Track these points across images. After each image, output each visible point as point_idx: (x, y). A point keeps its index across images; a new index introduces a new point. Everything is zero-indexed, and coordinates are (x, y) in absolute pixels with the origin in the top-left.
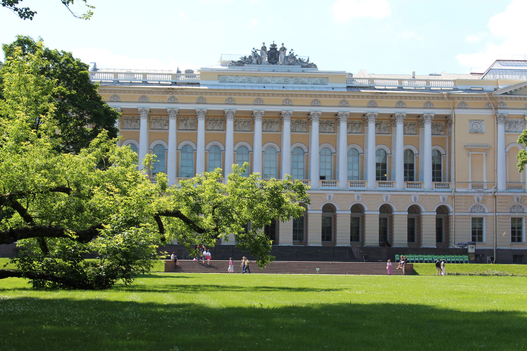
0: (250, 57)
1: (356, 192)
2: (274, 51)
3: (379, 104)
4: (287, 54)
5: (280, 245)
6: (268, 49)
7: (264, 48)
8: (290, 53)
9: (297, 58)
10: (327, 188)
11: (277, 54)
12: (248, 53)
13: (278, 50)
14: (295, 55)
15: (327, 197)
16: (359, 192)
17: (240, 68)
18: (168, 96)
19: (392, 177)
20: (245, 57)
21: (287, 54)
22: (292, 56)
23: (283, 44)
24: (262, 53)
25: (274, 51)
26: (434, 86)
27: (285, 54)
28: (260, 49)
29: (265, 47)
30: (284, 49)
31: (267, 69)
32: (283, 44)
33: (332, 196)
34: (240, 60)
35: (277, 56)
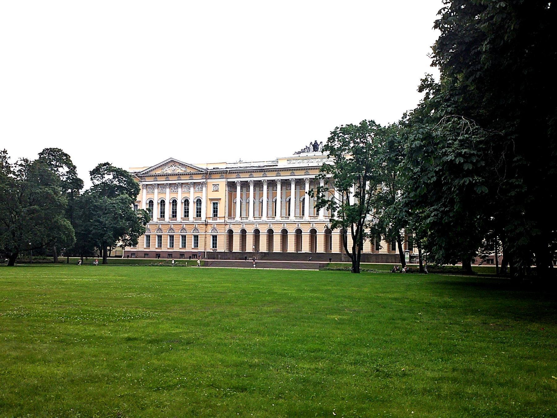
7: (311, 143)
13: (319, 143)
17: (298, 155)
19: (235, 215)
31: (312, 154)
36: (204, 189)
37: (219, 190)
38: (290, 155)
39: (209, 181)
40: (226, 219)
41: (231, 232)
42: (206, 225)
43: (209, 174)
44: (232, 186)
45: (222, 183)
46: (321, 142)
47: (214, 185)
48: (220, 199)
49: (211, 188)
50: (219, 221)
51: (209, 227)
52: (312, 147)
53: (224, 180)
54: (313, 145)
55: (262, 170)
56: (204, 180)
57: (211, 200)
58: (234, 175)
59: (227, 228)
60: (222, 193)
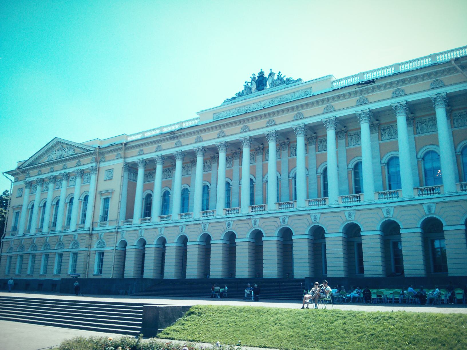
0: (243, 92)
3: (370, 100)
4: (276, 77)
5: (236, 278)
6: (257, 78)
7: (253, 79)
8: (278, 76)
9: (285, 79)
10: (315, 207)
11: (264, 81)
12: (241, 88)
13: (266, 75)
16: (349, 208)
18: (175, 141)
20: (239, 93)
22: (280, 78)
25: (261, 78)
26: (440, 59)
27: (273, 77)
28: (250, 80)
29: (254, 78)
33: (318, 216)
34: (235, 96)
35: (264, 82)
36: (93, 177)
37: (113, 178)
39: (102, 165)
40: (121, 224)
41: (124, 244)
42: (91, 235)
43: (100, 153)
44: (131, 169)
45: (116, 165)
47: (110, 171)
48: (112, 192)
49: (103, 175)
51: (95, 238)
54: (256, 83)
55: (173, 135)
56: (94, 164)
57: (102, 194)
59: (120, 238)
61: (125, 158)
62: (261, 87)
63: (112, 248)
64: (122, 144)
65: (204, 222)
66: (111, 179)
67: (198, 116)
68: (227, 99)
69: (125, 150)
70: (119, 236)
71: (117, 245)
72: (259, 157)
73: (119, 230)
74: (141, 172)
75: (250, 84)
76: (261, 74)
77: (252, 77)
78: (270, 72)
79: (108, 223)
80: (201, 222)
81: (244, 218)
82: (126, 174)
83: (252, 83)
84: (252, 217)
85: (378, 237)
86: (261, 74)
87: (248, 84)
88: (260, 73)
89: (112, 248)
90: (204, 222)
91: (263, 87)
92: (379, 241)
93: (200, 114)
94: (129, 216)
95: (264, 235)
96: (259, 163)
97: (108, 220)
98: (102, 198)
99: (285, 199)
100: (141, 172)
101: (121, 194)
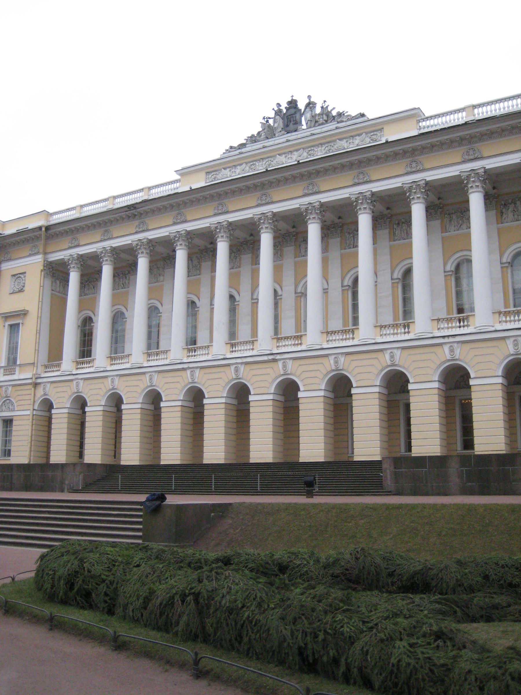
0: (259, 133)
1: (446, 340)
2: (292, 111)
4: (318, 110)
6: (285, 111)
7: (278, 112)
8: (322, 107)
9: (334, 113)
12: (256, 129)
13: (301, 106)
14: (329, 109)
15: (387, 357)
18: (136, 223)
21: (318, 110)
23: (309, 97)
24: (275, 122)
25: (292, 111)
28: (272, 114)
29: (280, 111)
30: (311, 105)
32: (309, 97)
34: (245, 142)
38: (218, 157)
40: (40, 370)
44: (57, 272)
46: (311, 105)
47: (18, 276)
48: (24, 313)
50: (20, 375)
52: (280, 123)
53: (39, 259)
58: (65, 242)
60: (33, 297)
61: (45, 253)
62: (292, 127)
63: (28, 412)
64: (40, 228)
65: (191, 365)
66: (21, 291)
67: (178, 177)
68: (231, 147)
69: (47, 238)
70: (40, 392)
71: (36, 408)
72: (289, 251)
73: (39, 381)
74: (74, 278)
75: (271, 122)
76: (293, 104)
77: (276, 109)
78: (308, 101)
79: (17, 369)
80: (185, 366)
81: (265, 358)
82: (48, 282)
83: (274, 118)
84: (278, 357)
85: (500, 387)
86: (293, 104)
87: (267, 121)
88: (290, 103)
89: (28, 412)
90: (191, 365)
91: (295, 126)
92: (500, 393)
93: (180, 175)
94: (55, 355)
95: (302, 388)
96: (289, 262)
97: (18, 363)
98: (7, 324)
99: (336, 324)
100: (74, 278)
101: (39, 318)
